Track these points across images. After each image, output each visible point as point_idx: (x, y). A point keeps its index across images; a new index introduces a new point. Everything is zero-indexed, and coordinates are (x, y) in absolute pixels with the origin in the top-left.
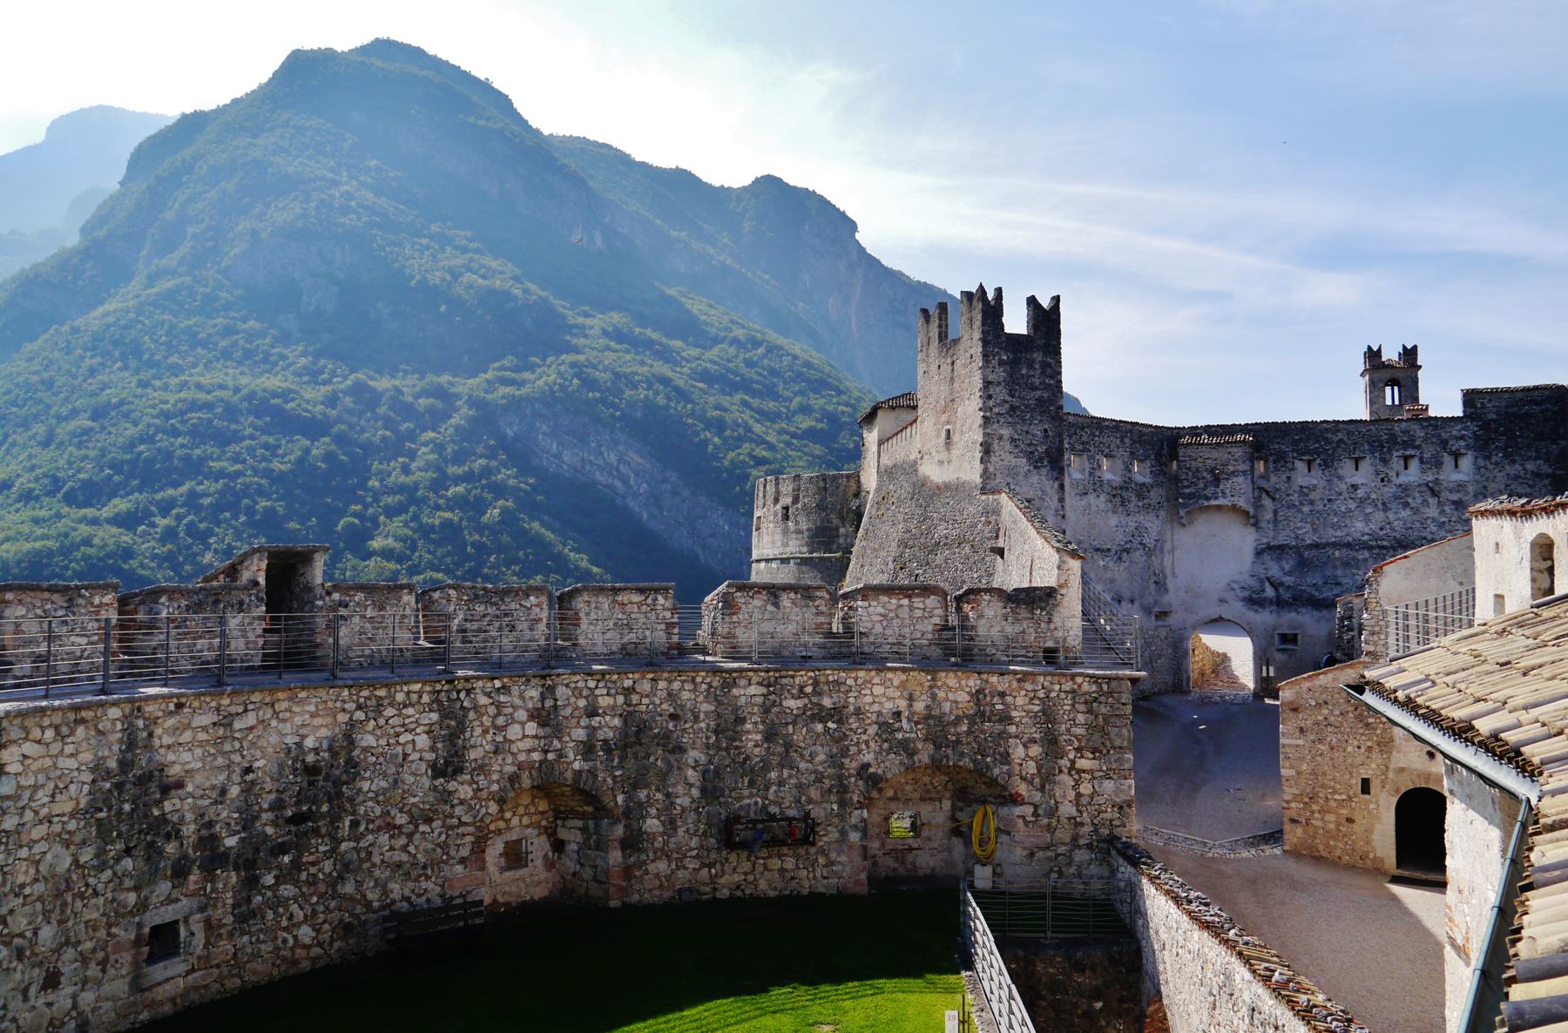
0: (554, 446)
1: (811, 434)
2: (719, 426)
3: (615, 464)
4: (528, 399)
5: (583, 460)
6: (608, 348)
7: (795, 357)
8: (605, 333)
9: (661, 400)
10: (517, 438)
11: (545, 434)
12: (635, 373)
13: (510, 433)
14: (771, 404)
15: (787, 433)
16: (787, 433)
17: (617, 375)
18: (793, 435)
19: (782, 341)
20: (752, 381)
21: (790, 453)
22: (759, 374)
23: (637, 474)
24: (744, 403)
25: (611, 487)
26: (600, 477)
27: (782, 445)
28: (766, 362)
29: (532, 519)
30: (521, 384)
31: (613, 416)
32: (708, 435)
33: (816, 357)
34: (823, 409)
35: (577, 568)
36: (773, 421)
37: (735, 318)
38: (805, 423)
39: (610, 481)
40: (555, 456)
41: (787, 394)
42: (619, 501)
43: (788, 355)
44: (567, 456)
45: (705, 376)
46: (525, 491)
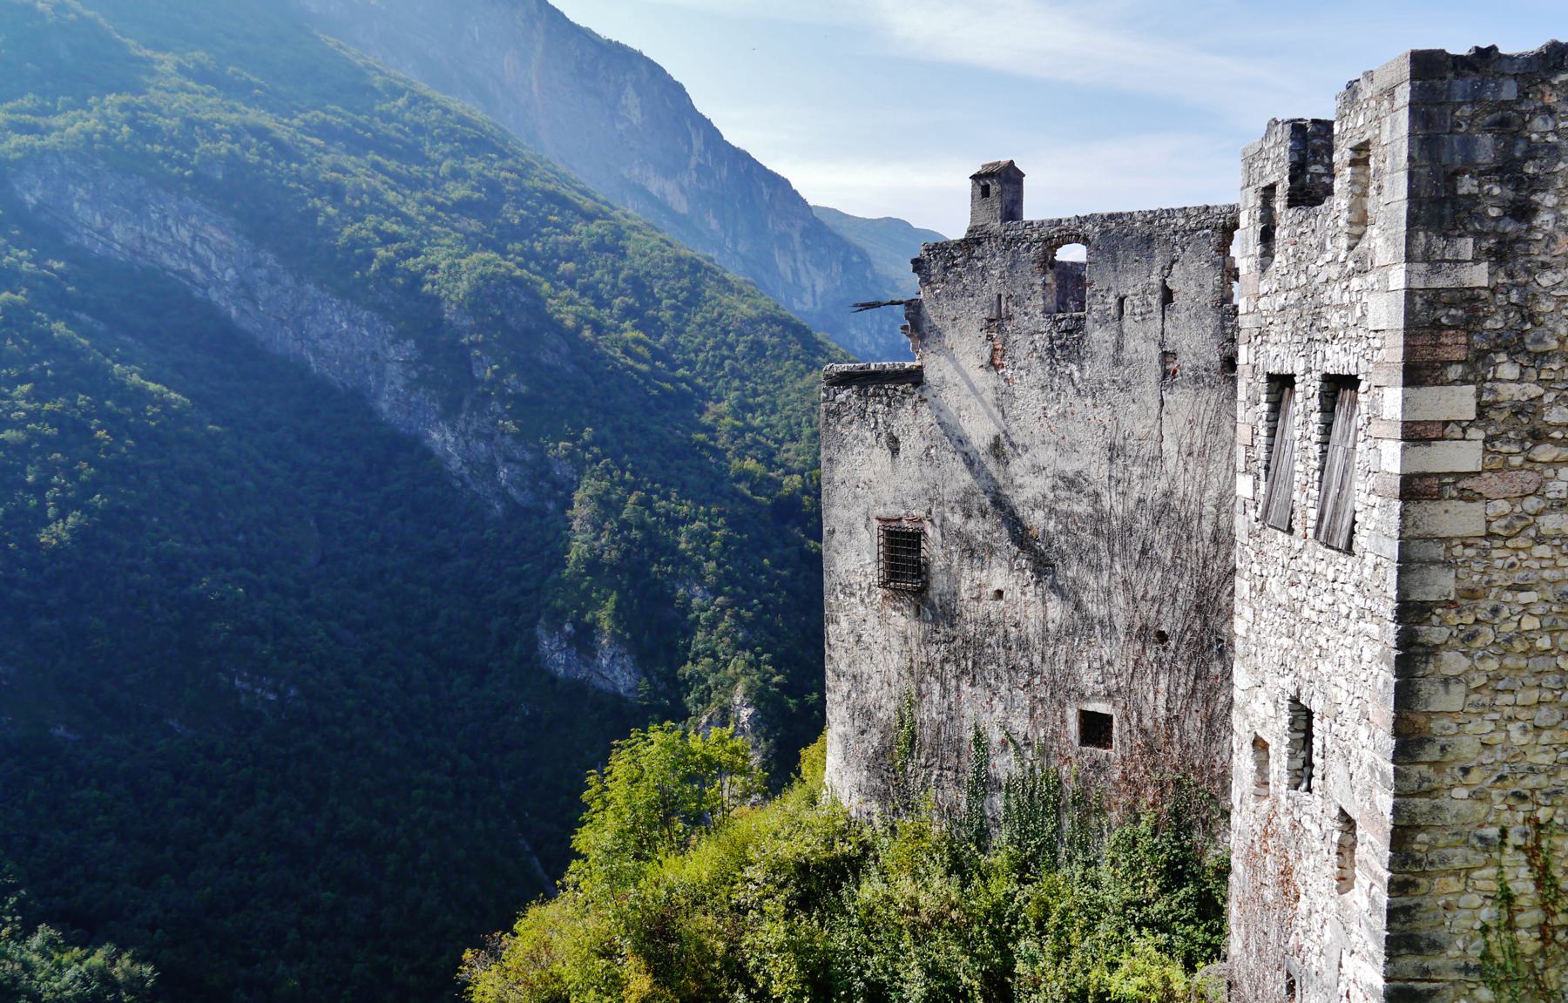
0: (98, 218)
1: (464, 207)
2: (336, 193)
3: (188, 242)
4: (55, 153)
5: (142, 237)
6: (183, 89)
7: (446, 111)
8: (181, 69)
9: (252, 157)
10: (41, 206)
11: (82, 201)
12: (218, 121)
13: (30, 199)
14: (415, 169)
15: (432, 203)
16: (432, 203)
17: (190, 123)
18: (440, 207)
19: (437, 95)
20: (388, 138)
21: (435, 228)
22: (399, 130)
23: (219, 257)
24: (376, 166)
25: (187, 275)
26: (168, 260)
27: (422, 218)
28: (408, 116)
29: (54, 318)
30: (49, 129)
31: (182, 177)
32: (318, 203)
33: (478, 115)
34: (480, 174)
35: (122, 385)
36: (413, 189)
37: (372, 62)
38: (458, 191)
39: (184, 266)
40: (100, 232)
41: (434, 156)
42: (198, 293)
43: (437, 108)
44: (118, 231)
45: (327, 132)
46: (47, 280)
